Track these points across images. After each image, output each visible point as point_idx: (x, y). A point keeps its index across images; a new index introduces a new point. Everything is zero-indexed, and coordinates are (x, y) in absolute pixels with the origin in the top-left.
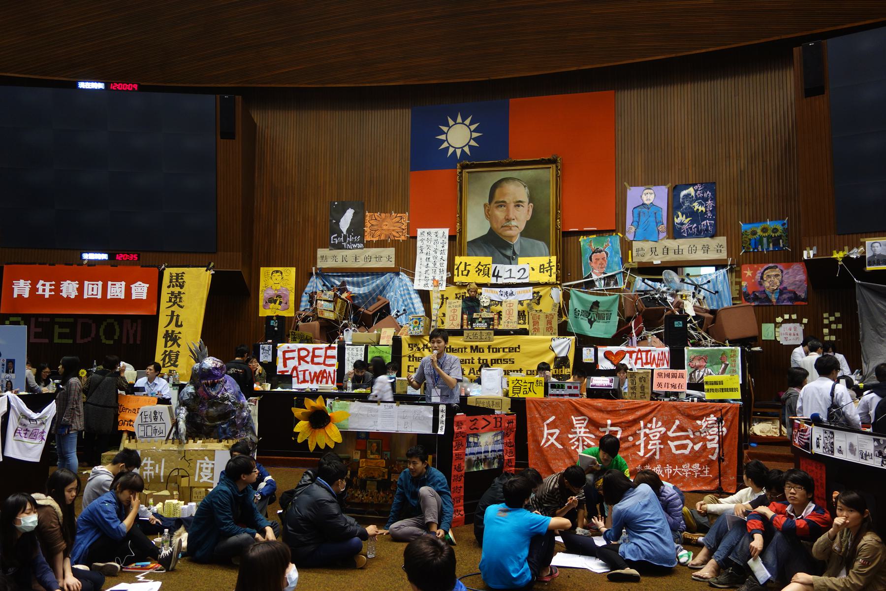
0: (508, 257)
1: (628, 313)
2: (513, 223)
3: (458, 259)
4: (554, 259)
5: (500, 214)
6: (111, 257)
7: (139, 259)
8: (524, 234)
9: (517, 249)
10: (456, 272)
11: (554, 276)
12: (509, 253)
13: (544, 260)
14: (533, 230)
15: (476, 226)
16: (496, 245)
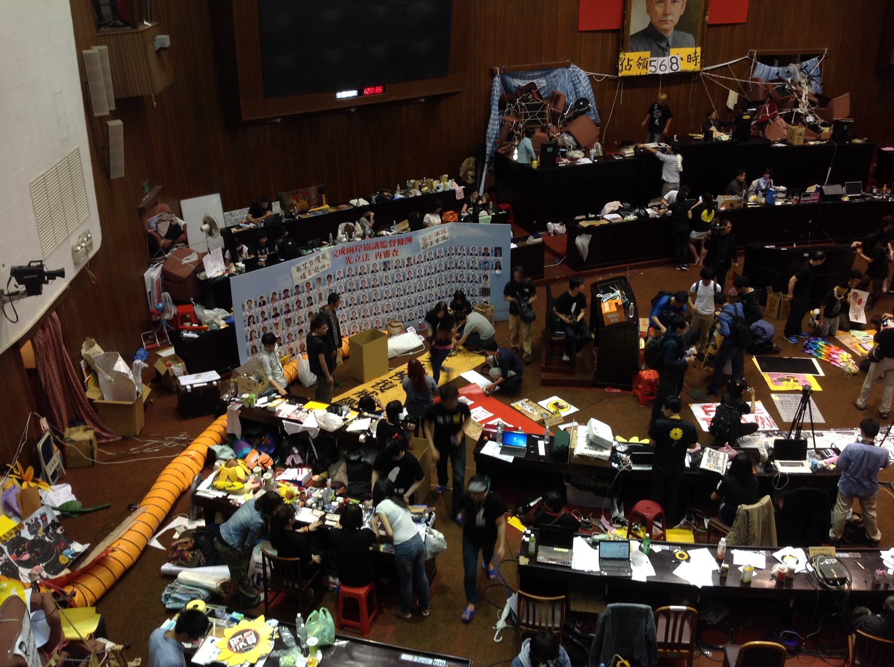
0: (663, 49)
1: (761, 98)
2: (670, 18)
3: (622, 56)
4: (699, 49)
5: (659, 9)
6: (360, 93)
7: (384, 91)
8: (678, 27)
9: (670, 40)
10: (620, 68)
11: (699, 65)
12: (664, 45)
13: (690, 51)
14: (683, 25)
15: (638, 23)
16: (654, 40)
